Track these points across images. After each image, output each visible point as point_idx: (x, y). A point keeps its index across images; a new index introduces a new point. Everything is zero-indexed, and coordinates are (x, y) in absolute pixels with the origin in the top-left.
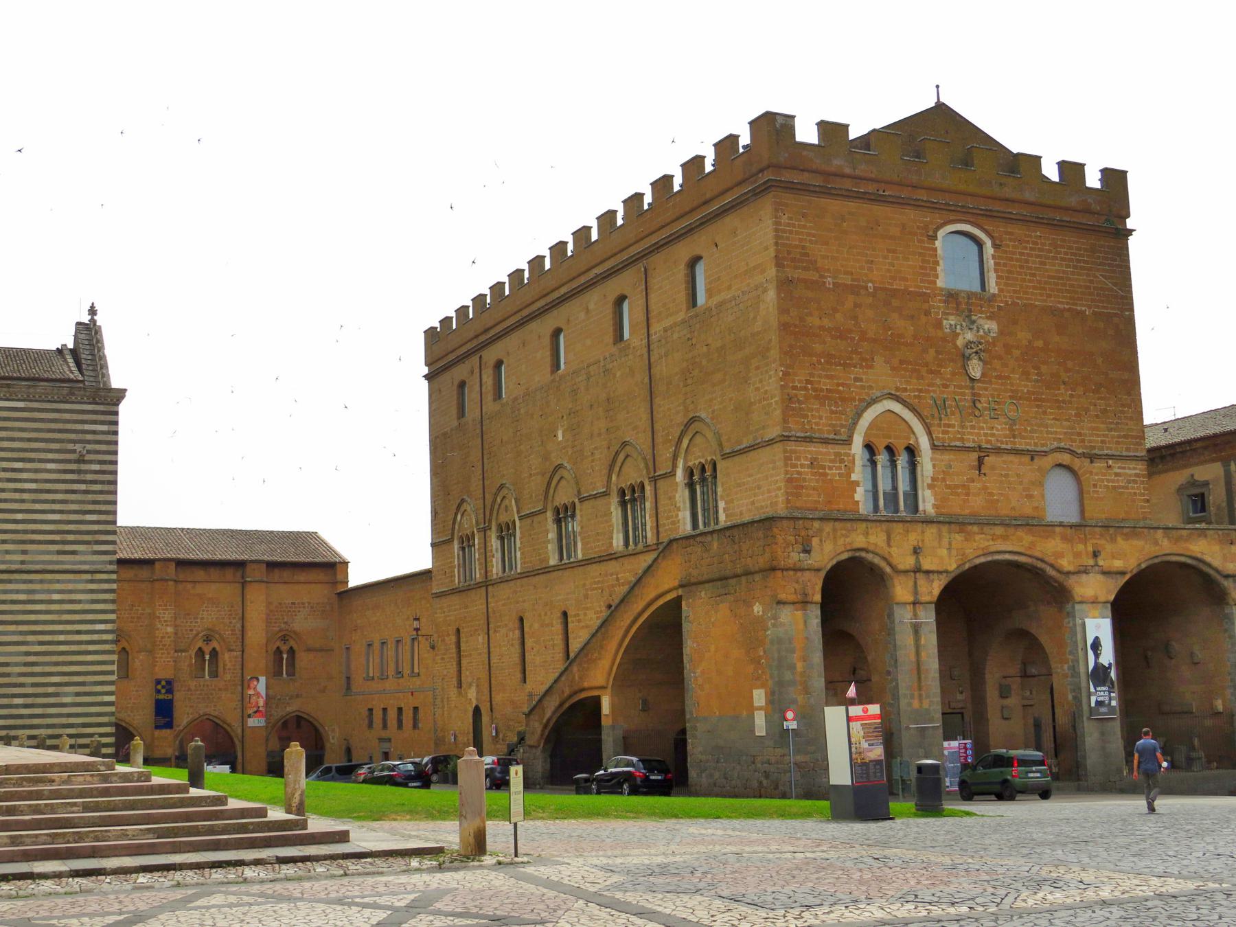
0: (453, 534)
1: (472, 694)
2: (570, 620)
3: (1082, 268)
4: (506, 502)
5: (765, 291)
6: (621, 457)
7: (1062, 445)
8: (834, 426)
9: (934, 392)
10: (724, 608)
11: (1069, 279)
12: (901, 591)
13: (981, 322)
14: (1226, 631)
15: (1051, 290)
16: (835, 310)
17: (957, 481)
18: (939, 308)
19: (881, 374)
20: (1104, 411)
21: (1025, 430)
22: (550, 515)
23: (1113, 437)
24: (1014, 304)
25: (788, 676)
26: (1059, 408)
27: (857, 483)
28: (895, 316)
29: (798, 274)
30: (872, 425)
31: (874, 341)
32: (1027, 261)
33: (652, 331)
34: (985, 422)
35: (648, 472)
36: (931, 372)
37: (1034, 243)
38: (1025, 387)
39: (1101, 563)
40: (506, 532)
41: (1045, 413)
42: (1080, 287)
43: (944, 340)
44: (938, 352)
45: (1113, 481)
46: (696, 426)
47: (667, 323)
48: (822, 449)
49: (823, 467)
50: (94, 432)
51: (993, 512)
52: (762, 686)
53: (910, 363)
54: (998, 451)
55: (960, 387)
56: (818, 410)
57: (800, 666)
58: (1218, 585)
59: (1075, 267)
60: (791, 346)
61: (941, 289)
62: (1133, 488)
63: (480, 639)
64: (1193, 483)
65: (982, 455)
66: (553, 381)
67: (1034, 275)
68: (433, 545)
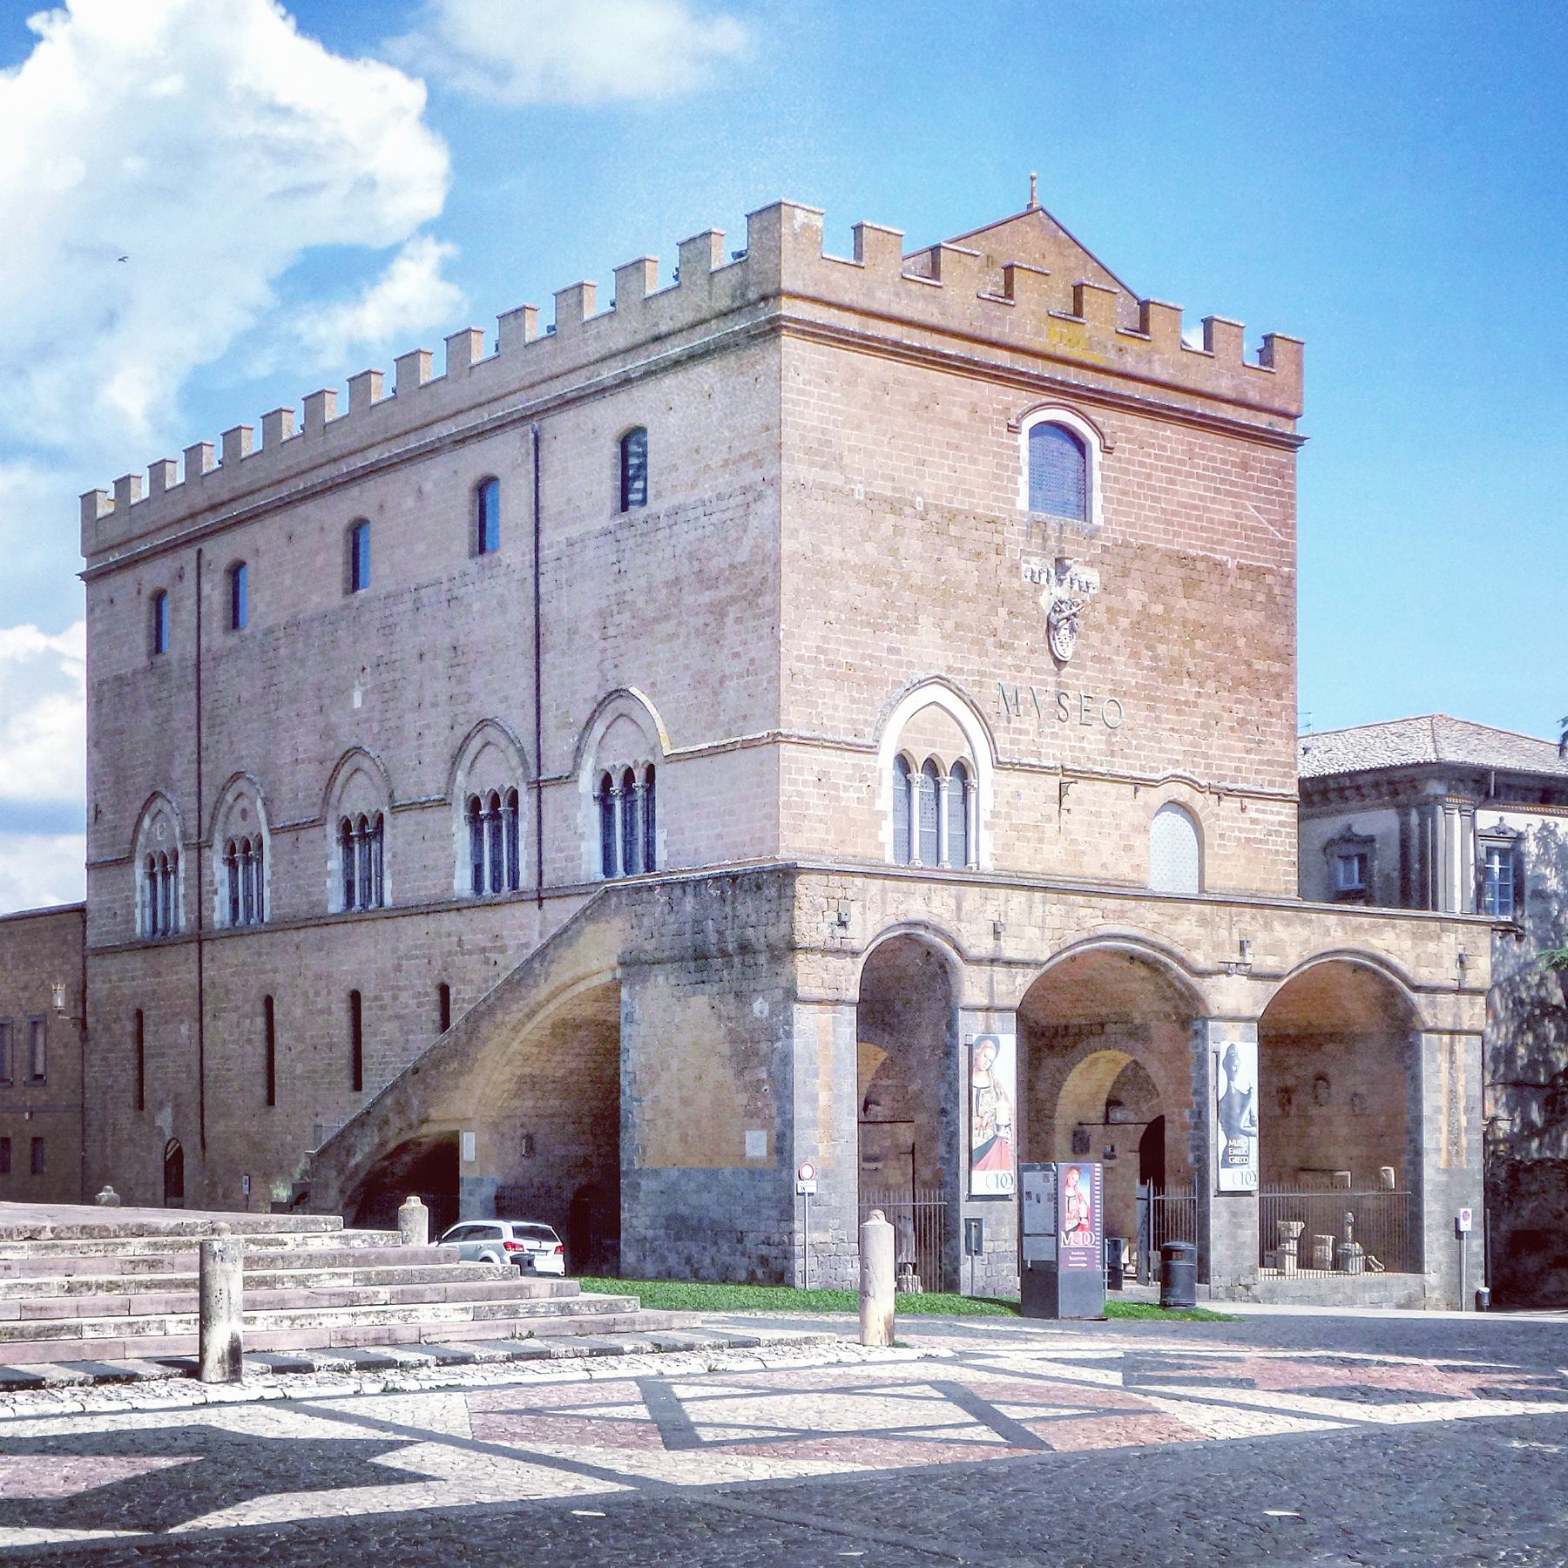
0: (132, 851)
1: (165, 1119)
2: (364, 1004)
4: (244, 803)
5: (760, 497)
6: (476, 744)
7: (1179, 772)
8: (855, 722)
9: (1003, 676)
10: (700, 1003)
11: (1206, 509)
12: (972, 987)
14: (1408, 1068)
15: (1181, 525)
17: (1027, 818)
19: (927, 647)
20: (1242, 722)
22: (332, 830)
27: (882, 815)
28: (952, 551)
31: (920, 589)
32: (1149, 476)
33: (543, 541)
35: (526, 775)
39: (1249, 959)
40: (243, 854)
41: (1158, 719)
42: (1222, 523)
43: (1021, 594)
45: (1248, 831)
46: (619, 704)
47: (574, 531)
49: (836, 787)
51: (1075, 870)
52: (763, 1127)
56: (832, 696)
57: (824, 1098)
58: (1406, 1000)
59: (1217, 490)
61: (1022, 513)
63: (184, 1029)
64: (1348, 838)
65: (1069, 775)
66: (347, 607)
67: (1156, 500)
68: (91, 866)
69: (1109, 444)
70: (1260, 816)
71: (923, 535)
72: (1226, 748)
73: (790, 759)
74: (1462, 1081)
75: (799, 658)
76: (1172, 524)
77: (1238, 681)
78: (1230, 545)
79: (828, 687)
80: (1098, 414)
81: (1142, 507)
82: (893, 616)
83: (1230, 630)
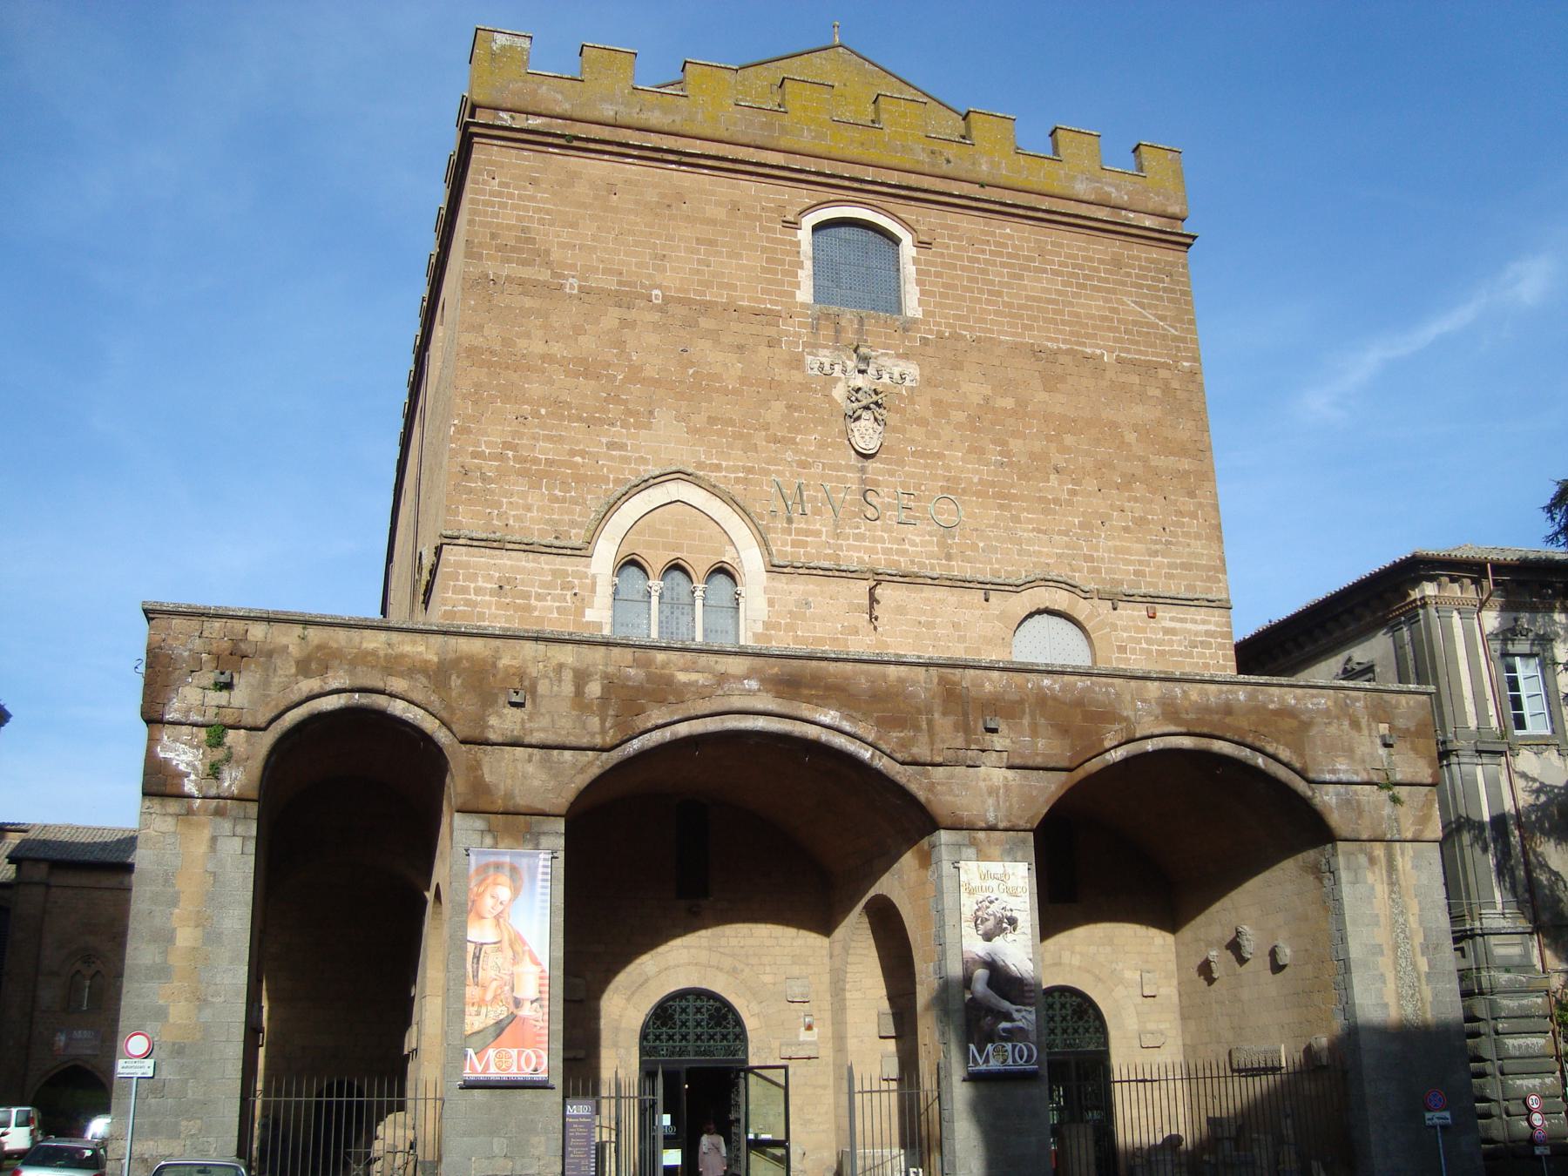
3: (1094, 288)
8: (556, 523)
9: (778, 472)
13: (882, 361)
15: (1035, 319)
16: (578, 330)
18: (799, 335)
20: (1141, 522)
21: (974, 547)
23: (1159, 566)
24: (956, 337)
26: (1046, 511)
28: (706, 344)
29: (506, 270)
31: (656, 383)
32: (984, 272)
34: (889, 530)
37: (997, 244)
38: (974, 472)
42: (1092, 317)
43: (806, 387)
44: (789, 407)
49: (527, 596)
53: (731, 422)
54: (908, 579)
55: (837, 468)
56: (523, 495)
57: (185, 937)
59: (1079, 286)
60: (478, 386)
61: (803, 305)
62: (1202, 655)
65: (878, 577)
69: (923, 238)
70: (1178, 625)
71: (656, 327)
72: (1117, 550)
73: (458, 564)
74: (1414, 907)
75: (475, 455)
76: (1021, 317)
77: (1129, 480)
78: (1103, 339)
79: (521, 486)
80: (910, 212)
81: (979, 300)
82: (614, 410)
83: (1114, 425)
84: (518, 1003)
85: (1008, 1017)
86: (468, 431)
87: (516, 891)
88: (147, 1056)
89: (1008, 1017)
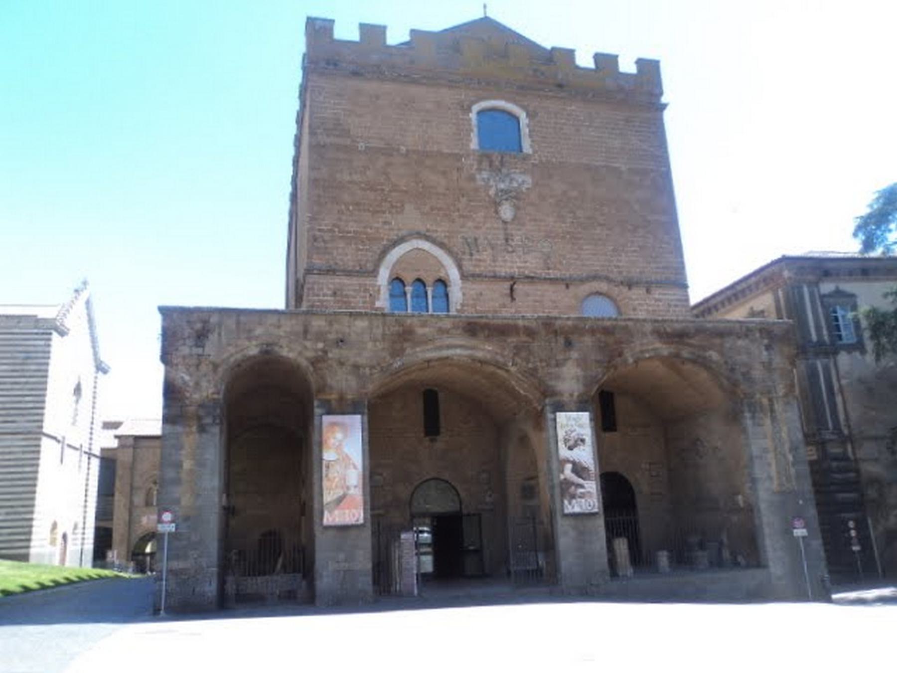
21: (561, 263)
25: (171, 474)
30: (399, 262)
31: (406, 192)
36: (461, 216)
48: (346, 280)
49: (347, 296)
50: (34, 346)
53: (440, 209)
54: (531, 279)
57: (187, 465)
61: (474, 150)
65: (513, 280)
75: (320, 230)
79: (341, 245)
84: (348, 488)
85: (582, 486)
86: (316, 219)
87: (345, 436)
88: (172, 522)
89: (582, 486)
